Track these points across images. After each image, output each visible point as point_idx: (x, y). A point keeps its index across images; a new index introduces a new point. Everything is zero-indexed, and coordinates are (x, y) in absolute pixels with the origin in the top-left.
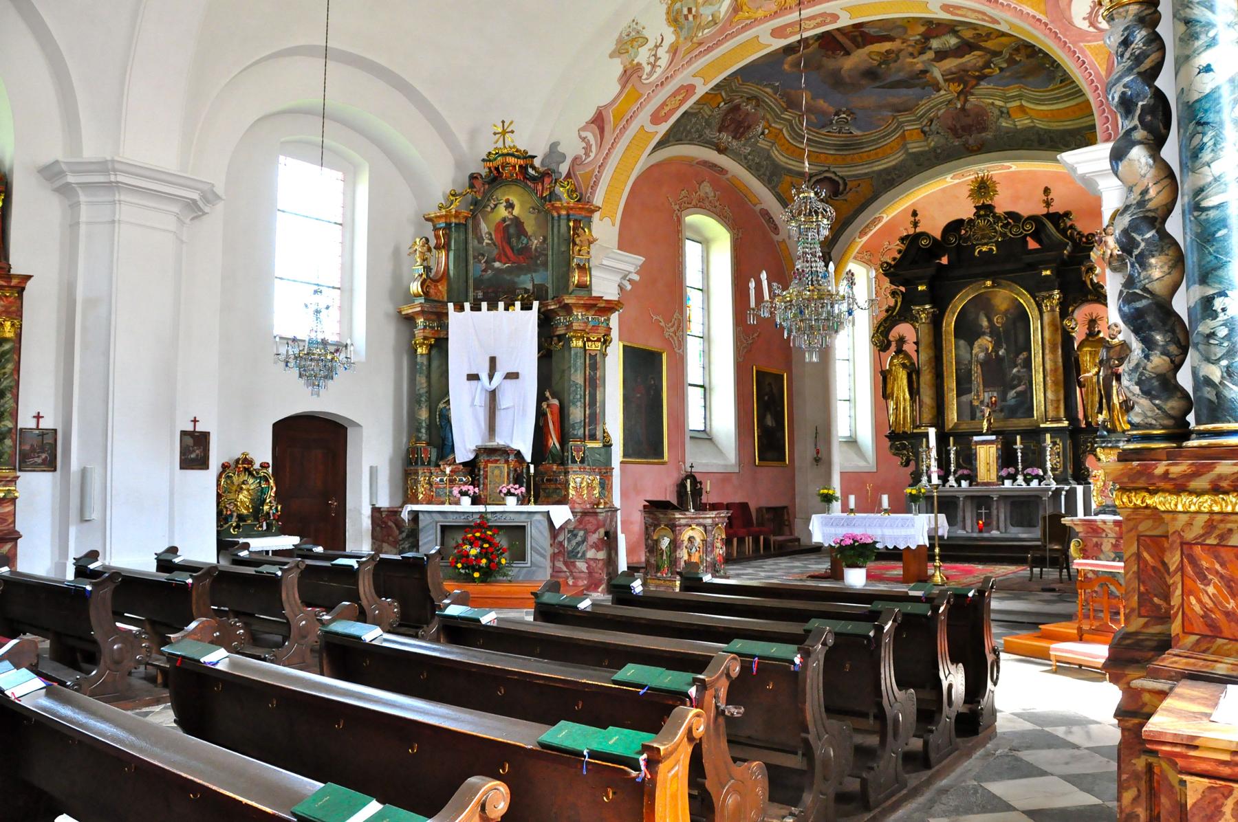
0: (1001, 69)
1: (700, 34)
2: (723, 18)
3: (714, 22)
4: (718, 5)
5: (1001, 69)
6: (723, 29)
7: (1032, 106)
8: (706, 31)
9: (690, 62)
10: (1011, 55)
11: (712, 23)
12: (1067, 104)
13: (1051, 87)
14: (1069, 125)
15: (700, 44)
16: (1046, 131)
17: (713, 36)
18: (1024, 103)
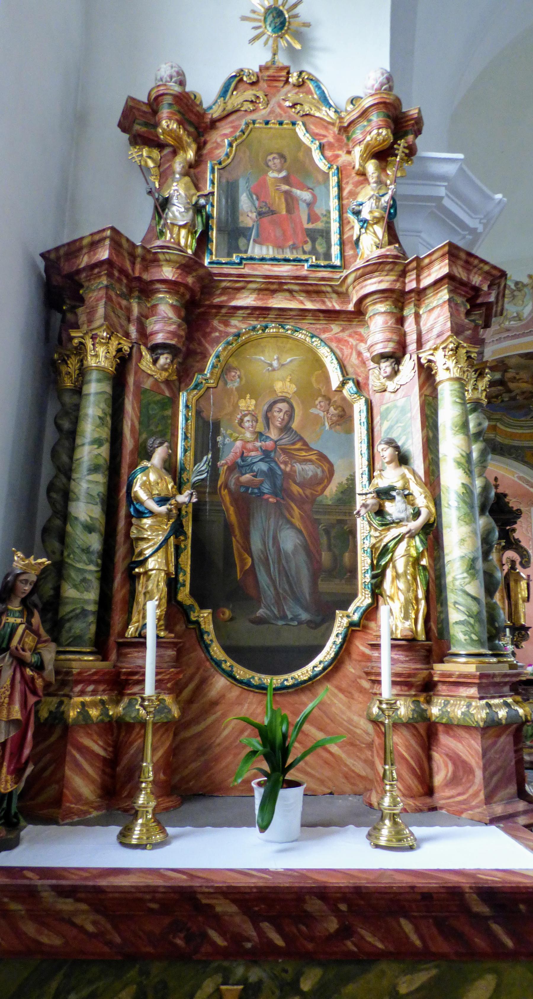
0: (502, 401)
1: (507, 323)
2: (526, 318)
3: (519, 318)
4: (522, 308)
5: (502, 401)
6: (526, 326)
7: (502, 427)
8: (512, 322)
9: (499, 340)
10: (517, 394)
11: (517, 319)
12: (525, 431)
13: (523, 419)
14: (516, 443)
15: (508, 330)
16: (500, 443)
17: (517, 329)
18: (499, 425)
